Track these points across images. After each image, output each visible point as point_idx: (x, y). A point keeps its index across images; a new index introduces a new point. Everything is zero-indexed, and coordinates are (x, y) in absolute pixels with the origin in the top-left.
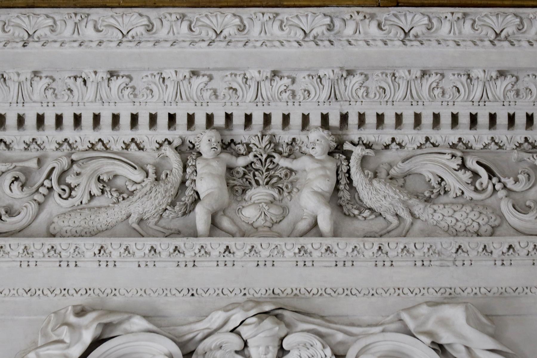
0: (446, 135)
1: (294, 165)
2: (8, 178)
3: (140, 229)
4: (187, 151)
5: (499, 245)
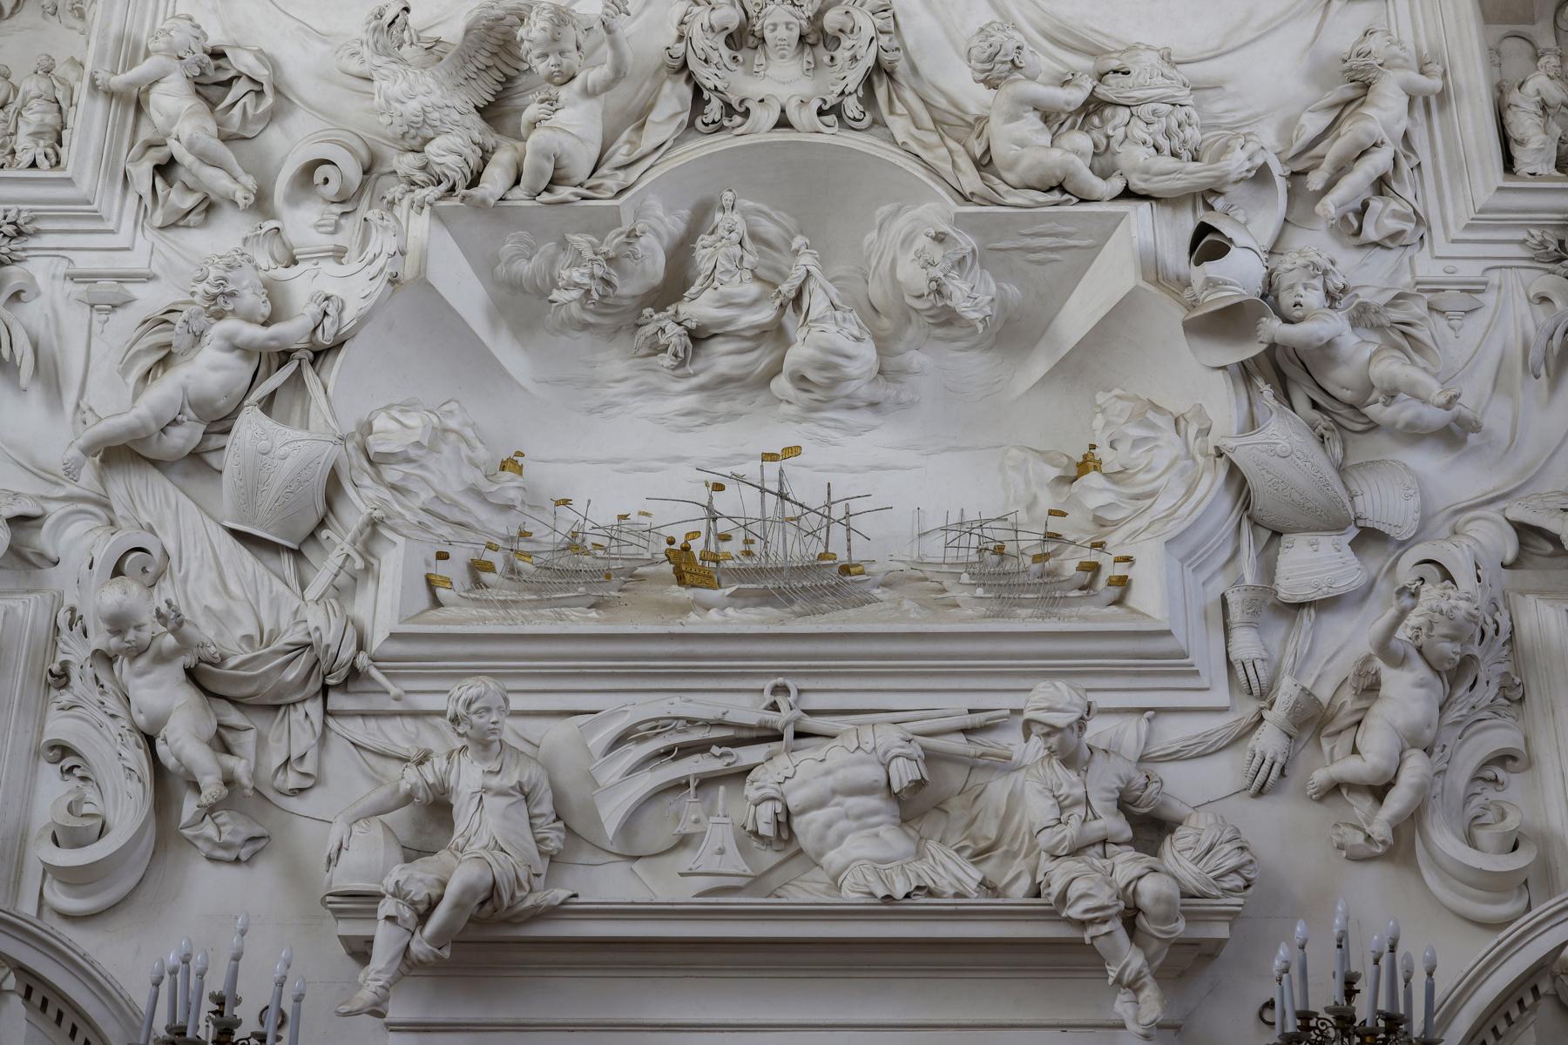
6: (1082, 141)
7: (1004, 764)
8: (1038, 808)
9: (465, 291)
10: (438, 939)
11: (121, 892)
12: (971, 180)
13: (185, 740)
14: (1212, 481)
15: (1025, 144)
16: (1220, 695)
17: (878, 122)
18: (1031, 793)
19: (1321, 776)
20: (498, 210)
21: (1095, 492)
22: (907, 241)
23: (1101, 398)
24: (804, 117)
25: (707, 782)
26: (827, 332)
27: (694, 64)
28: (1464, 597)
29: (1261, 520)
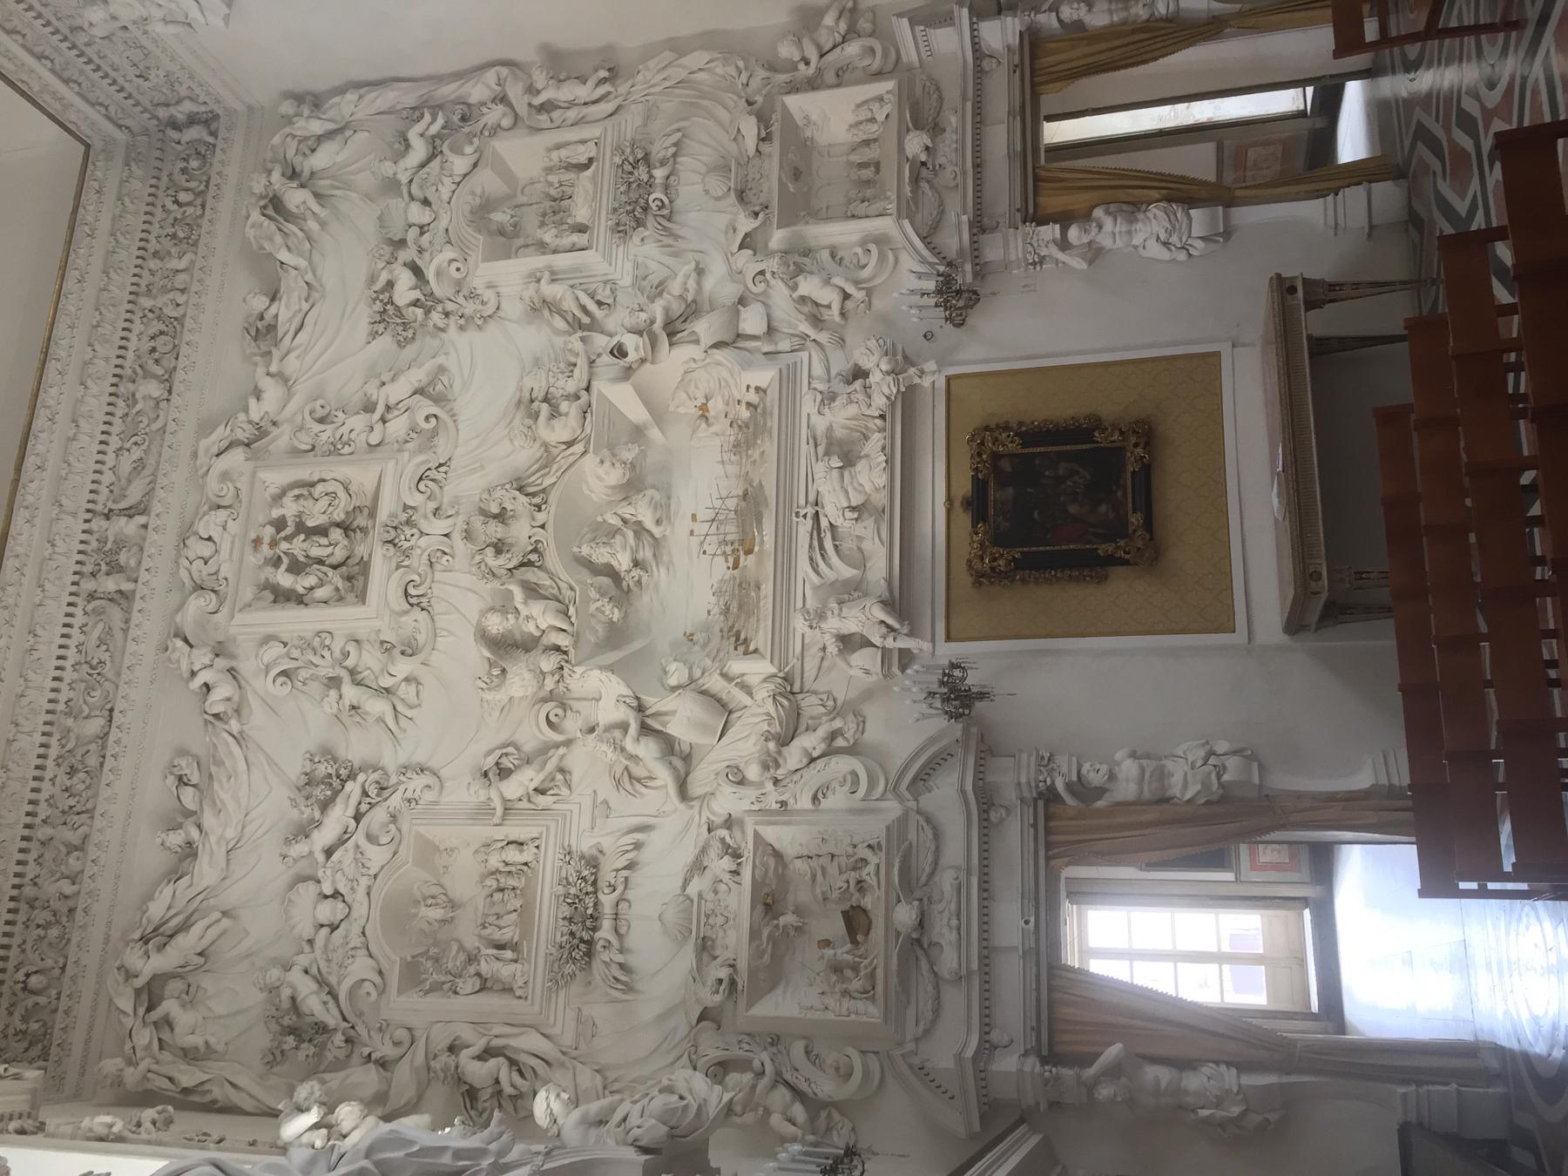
0: (110, 459)
1: (111, 539)
2: (88, 699)
4: (92, 596)
5: (172, 426)
7: (830, 429)
8: (853, 410)
10: (902, 625)
12: (578, 448)
14: (718, 355)
15: (559, 432)
16: (804, 355)
17: (543, 491)
18: (841, 417)
19: (837, 319)
21: (716, 406)
22: (600, 479)
23: (671, 409)
24: (541, 517)
25: (834, 539)
27: (510, 566)
28: (773, 264)
29: (732, 340)
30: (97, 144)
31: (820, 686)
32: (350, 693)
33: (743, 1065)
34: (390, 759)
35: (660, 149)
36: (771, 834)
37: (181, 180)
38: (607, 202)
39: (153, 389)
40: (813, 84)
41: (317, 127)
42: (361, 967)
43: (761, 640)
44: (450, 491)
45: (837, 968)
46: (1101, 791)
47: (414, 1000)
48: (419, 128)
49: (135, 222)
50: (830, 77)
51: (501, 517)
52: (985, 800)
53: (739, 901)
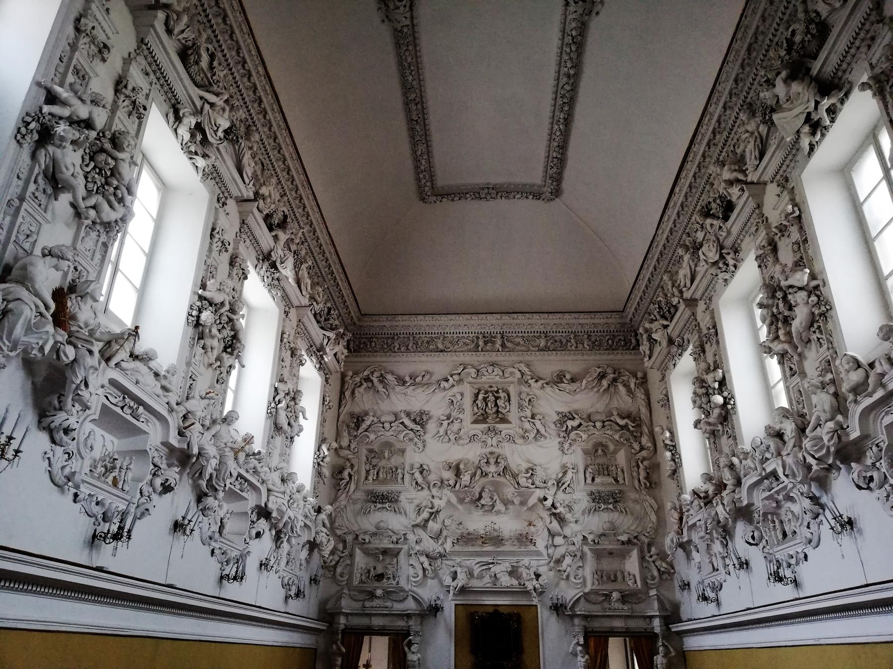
3: (469, 351)
4: (478, 338)
6: (530, 481)
9: (454, 500)
11: (420, 584)
13: (426, 565)
14: (546, 530)
16: (546, 558)
20: (458, 491)
24: (495, 475)
26: (499, 506)
29: (552, 535)
30: (624, 315)
31: (443, 566)
32: (445, 423)
33: (345, 548)
34: (428, 437)
35: (620, 506)
36: (402, 553)
37: (616, 340)
38: (601, 489)
39: (543, 343)
40: (642, 559)
41: (632, 386)
42: (372, 437)
43: (457, 548)
44: (505, 444)
45: (369, 571)
46: (409, 649)
47: (364, 452)
48: (629, 422)
49: (600, 328)
50: (644, 565)
51: (497, 463)
52: (409, 616)
53: (386, 544)
